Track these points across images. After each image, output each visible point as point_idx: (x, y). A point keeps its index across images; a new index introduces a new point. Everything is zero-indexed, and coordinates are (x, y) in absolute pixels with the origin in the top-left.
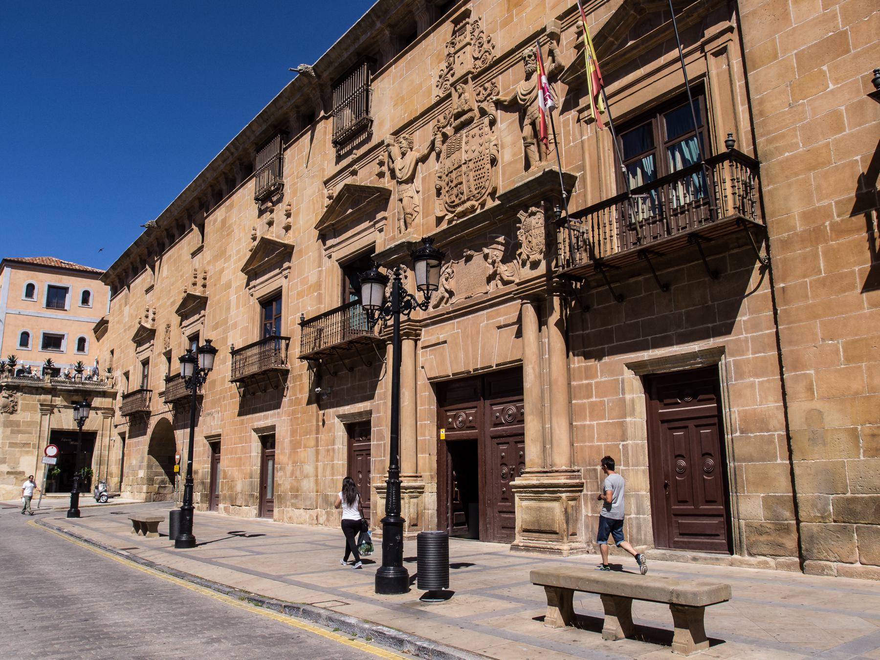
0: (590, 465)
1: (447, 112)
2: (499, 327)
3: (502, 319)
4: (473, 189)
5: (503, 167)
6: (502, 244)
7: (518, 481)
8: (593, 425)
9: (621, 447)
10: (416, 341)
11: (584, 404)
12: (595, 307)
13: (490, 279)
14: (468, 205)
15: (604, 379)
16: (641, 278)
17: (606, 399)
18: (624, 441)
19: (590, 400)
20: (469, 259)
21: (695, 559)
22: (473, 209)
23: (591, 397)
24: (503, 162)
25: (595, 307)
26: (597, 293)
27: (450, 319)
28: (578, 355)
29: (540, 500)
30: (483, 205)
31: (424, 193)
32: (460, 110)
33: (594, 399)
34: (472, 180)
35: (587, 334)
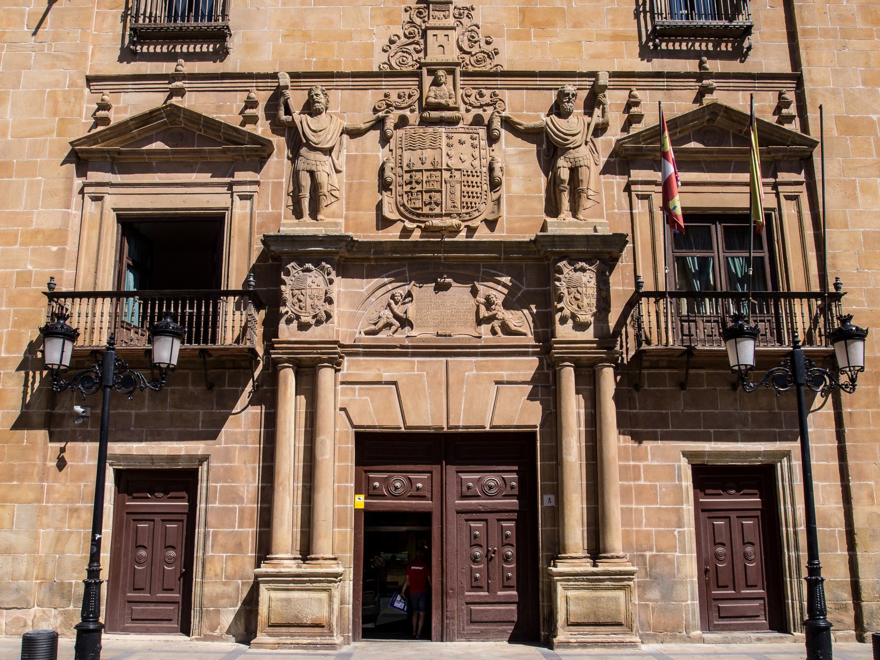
0: (637, 551)
1: (407, 92)
2: (497, 383)
3: (504, 373)
4: (458, 204)
5: (510, 198)
6: (505, 285)
7: (562, 567)
8: (640, 511)
9: (676, 533)
10: (337, 371)
11: (630, 487)
12: (646, 387)
13: (479, 322)
14: (448, 222)
15: (655, 463)
16: (703, 372)
19: (637, 483)
20: (446, 287)
21: (759, 640)
22: (456, 231)
23: (639, 479)
24: (508, 191)
25: (646, 387)
26: (648, 374)
27: (414, 355)
28: (624, 434)
30: (471, 231)
31: (350, 176)
32: (443, 101)
33: (642, 482)
34: (458, 194)
35: (635, 414)
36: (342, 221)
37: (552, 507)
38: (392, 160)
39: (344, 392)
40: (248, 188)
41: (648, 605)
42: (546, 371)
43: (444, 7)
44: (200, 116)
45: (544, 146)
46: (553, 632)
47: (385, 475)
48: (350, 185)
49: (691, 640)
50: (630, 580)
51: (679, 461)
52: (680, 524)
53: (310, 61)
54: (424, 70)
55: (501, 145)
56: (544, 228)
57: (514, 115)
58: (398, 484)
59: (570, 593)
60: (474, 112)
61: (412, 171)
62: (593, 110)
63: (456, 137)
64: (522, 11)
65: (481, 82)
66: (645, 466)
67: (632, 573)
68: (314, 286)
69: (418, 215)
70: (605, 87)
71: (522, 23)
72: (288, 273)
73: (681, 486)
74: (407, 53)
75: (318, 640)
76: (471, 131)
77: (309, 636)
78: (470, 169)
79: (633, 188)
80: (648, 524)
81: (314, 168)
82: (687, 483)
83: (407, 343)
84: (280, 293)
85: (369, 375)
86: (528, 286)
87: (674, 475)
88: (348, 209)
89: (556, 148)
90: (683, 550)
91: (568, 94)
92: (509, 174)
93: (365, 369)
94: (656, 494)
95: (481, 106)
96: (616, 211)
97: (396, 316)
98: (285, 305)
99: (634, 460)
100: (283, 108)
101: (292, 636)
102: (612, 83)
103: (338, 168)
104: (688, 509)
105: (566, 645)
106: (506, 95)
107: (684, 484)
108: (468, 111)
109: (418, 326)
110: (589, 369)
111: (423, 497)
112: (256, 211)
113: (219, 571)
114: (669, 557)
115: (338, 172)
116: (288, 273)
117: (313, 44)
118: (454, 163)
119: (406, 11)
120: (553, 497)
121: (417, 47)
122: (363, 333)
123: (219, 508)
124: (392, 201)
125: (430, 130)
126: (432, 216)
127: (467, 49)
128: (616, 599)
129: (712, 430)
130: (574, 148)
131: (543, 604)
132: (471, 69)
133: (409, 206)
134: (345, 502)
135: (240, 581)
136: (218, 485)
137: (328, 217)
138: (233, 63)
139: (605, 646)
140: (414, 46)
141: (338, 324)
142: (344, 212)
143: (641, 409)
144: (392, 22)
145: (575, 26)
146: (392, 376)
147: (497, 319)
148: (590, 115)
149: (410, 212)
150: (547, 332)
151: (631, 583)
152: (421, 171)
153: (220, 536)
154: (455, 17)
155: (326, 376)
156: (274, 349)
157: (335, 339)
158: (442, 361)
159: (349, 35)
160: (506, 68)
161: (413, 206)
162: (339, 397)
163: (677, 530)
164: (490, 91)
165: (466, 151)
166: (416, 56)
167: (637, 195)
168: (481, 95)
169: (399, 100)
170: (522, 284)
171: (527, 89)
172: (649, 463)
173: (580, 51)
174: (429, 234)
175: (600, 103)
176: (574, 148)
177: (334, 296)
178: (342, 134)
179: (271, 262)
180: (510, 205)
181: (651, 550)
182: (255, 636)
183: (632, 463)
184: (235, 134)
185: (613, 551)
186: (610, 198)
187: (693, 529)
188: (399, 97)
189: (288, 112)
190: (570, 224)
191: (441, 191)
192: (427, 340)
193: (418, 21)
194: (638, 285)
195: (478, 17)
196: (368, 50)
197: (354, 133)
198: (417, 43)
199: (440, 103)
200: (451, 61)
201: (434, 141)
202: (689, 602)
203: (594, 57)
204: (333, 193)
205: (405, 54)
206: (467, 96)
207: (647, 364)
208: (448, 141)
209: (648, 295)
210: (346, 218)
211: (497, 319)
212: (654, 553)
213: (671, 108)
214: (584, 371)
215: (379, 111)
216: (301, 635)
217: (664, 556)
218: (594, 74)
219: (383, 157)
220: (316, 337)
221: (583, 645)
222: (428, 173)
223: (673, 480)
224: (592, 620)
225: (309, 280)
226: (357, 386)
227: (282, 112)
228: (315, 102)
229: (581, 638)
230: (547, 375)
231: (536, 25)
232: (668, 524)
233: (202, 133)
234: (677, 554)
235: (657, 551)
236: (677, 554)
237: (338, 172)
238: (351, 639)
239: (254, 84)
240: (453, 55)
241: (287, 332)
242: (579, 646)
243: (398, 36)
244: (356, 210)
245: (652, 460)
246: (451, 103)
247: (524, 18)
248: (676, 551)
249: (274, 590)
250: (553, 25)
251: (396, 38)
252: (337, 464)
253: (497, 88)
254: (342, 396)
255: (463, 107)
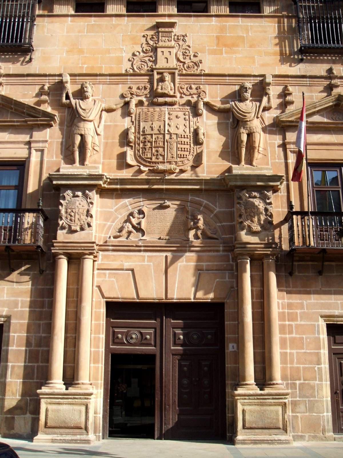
4: (175, 156)
7: (240, 391)
8: (293, 354)
9: (316, 369)
15: (302, 323)
17: (304, 336)
18: (319, 365)
24: (208, 148)
25: (297, 274)
29: (262, 405)
31: (106, 138)
32: (166, 92)
33: (294, 335)
36: (101, 166)
37: (235, 351)
38: (133, 128)
39: (99, 275)
40: (41, 145)
41: (297, 416)
42: (231, 263)
43: (168, 34)
44: (12, 99)
45: (231, 120)
46: (234, 433)
47: (125, 330)
48: (106, 144)
49: (326, 439)
50: (285, 398)
51: (318, 321)
52: (319, 363)
53: (83, 67)
54: (155, 72)
55: (203, 118)
56: (229, 170)
57: (212, 101)
58: (134, 336)
59: (247, 408)
60: (186, 98)
61: (146, 135)
62: (262, 98)
63: (174, 114)
64: (218, 38)
65: (190, 79)
66: (296, 325)
67: (287, 394)
68: (80, 207)
69: (149, 162)
70: (269, 84)
71: (218, 45)
72: (64, 198)
73: (319, 338)
74: (144, 62)
75: (78, 437)
76: (184, 110)
77: (72, 435)
78: (183, 134)
79: (288, 146)
80: (298, 362)
81: (83, 133)
82: (324, 336)
83: (140, 244)
84: (59, 211)
85: (115, 264)
86: (219, 208)
87: (315, 330)
88: (104, 158)
89: (238, 121)
90: (321, 380)
91: (246, 88)
92: (208, 137)
93: (113, 261)
94: (303, 343)
95: (190, 94)
96: (277, 161)
97: (133, 227)
98: (61, 219)
99: (289, 321)
100: (64, 95)
101: (61, 434)
102: (274, 82)
103: (99, 132)
104: (325, 352)
105: (243, 442)
106: (207, 88)
107: (321, 336)
108: (181, 97)
109: (148, 233)
110: (260, 261)
111: (149, 345)
112: (45, 159)
113: (14, 391)
114: (312, 384)
115: (98, 134)
116: (64, 198)
117: (85, 57)
118: (173, 130)
119: (144, 36)
120: (235, 345)
121: (151, 59)
122: (112, 238)
123: (16, 350)
124: (132, 153)
125: (157, 109)
126: (158, 163)
127: (182, 60)
128: (277, 412)
129: (339, 302)
130: (250, 121)
131: (229, 415)
132: (184, 72)
133: (143, 157)
134: (98, 347)
135: (28, 398)
136: (16, 335)
137: (91, 163)
138: (35, 67)
139: (269, 443)
140: (149, 58)
141: (96, 231)
142: (102, 160)
143: (293, 288)
144: (136, 44)
145: (251, 47)
146: (130, 265)
147: (200, 229)
148: (260, 101)
149: (144, 160)
150: (232, 237)
151: (286, 401)
152: (152, 135)
153: (16, 368)
154: (175, 41)
155: (88, 263)
156: (54, 247)
157: (93, 240)
158: (163, 256)
159: (108, 51)
160: (207, 72)
161: (146, 156)
162: (96, 279)
163: (317, 366)
164: (196, 86)
165: (181, 122)
166: (150, 64)
167: (291, 151)
168: (191, 88)
169: (138, 91)
170: (216, 206)
171: (220, 84)
172: (298, 323)
173: (254, 62)
174: (156, 174)
175: (267, 94)
176: (250, 121)
177: (93, 212)
178: (101, 111)
179: (53, 191)
180: (209, 157)
181: (300, 380)
182: (37, 434)
183: (287, 323)
184: (34, 111)
185: (275, 380)
186: (273, 153)
187: (327, 366)
188: (138, 88)
189: (67, 97)
190: (247, 169)
191: (164, 148)
192: (153, 242)
193: (151, 43)
194: (290, 206)
195: (189, 41)
196: (120, 60)
197: (109, 111)
198: (151, 56)
199: (165, 93)
200: (172, 67)
201: (160, 116)
202: (325, 414)
203: (263, 65)
204: (95, 148)
205: (143, 63)
206: (181, 88)
207: (297, 258)
208: (169, 116)
209: (297, 213)
210: (103, 164)
211: (200, 229)
212: (302, 381)
213: (311, 97)
214: (256, 262)
215: (125, 97)
216: (67, 434)
217: (308, 384)
218: (264, 76)
219: (127, 126)
220: (81, 239)
221: (255, 442)
222: (156, 136)
223: (314, 334)
224: (260, 426)
225: (77, 203)
226: (108, 272)
227: (64, 98)
228: (85, 92)
229: (253, 437)
230: (232, 265)
231: (225, 45)
232: (311, 363)
233: (13, 111)
234: (317, 382)
235: (304, 380)
236: (317, 382)
237: (98, 134)
238: (101, 437)
239: (47, 81)
240: (173, 63)
241: (61, 235)
242: (252, 443)
243: (139, 52)
244: (110, 159)
245: (301, 321)
246: (172, 93)
247: (218, 42)
248: (316, 380)
249: (50, 403)
250: (237, 46)
251: (138, 54)
252: (93, 322)
253: (201, 84)
254: (97, 277)
255: (178, 95)
